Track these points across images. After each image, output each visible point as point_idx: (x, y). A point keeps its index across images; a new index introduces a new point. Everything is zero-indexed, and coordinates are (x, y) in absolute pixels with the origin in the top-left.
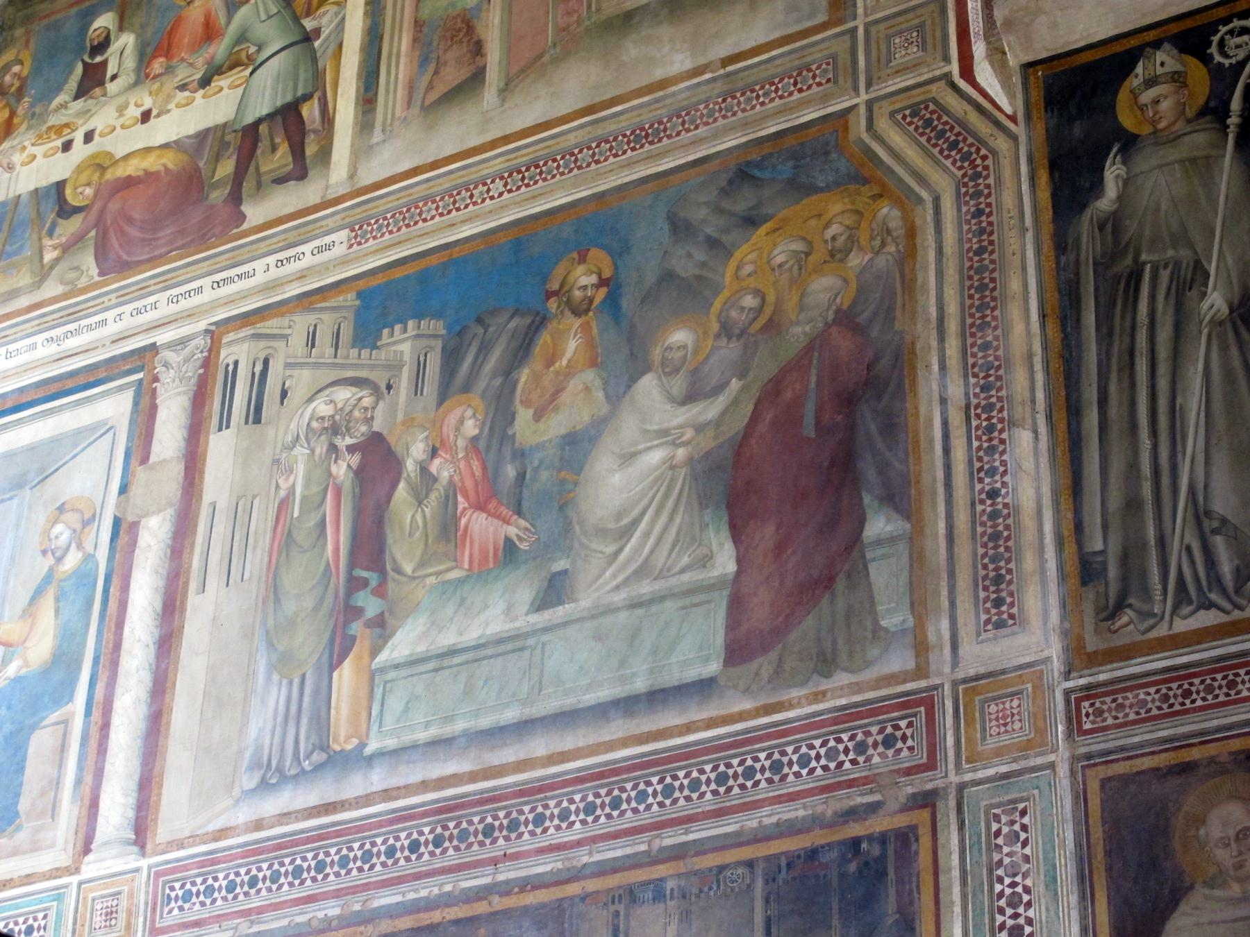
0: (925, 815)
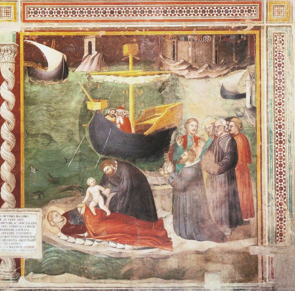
0: (257, 32)
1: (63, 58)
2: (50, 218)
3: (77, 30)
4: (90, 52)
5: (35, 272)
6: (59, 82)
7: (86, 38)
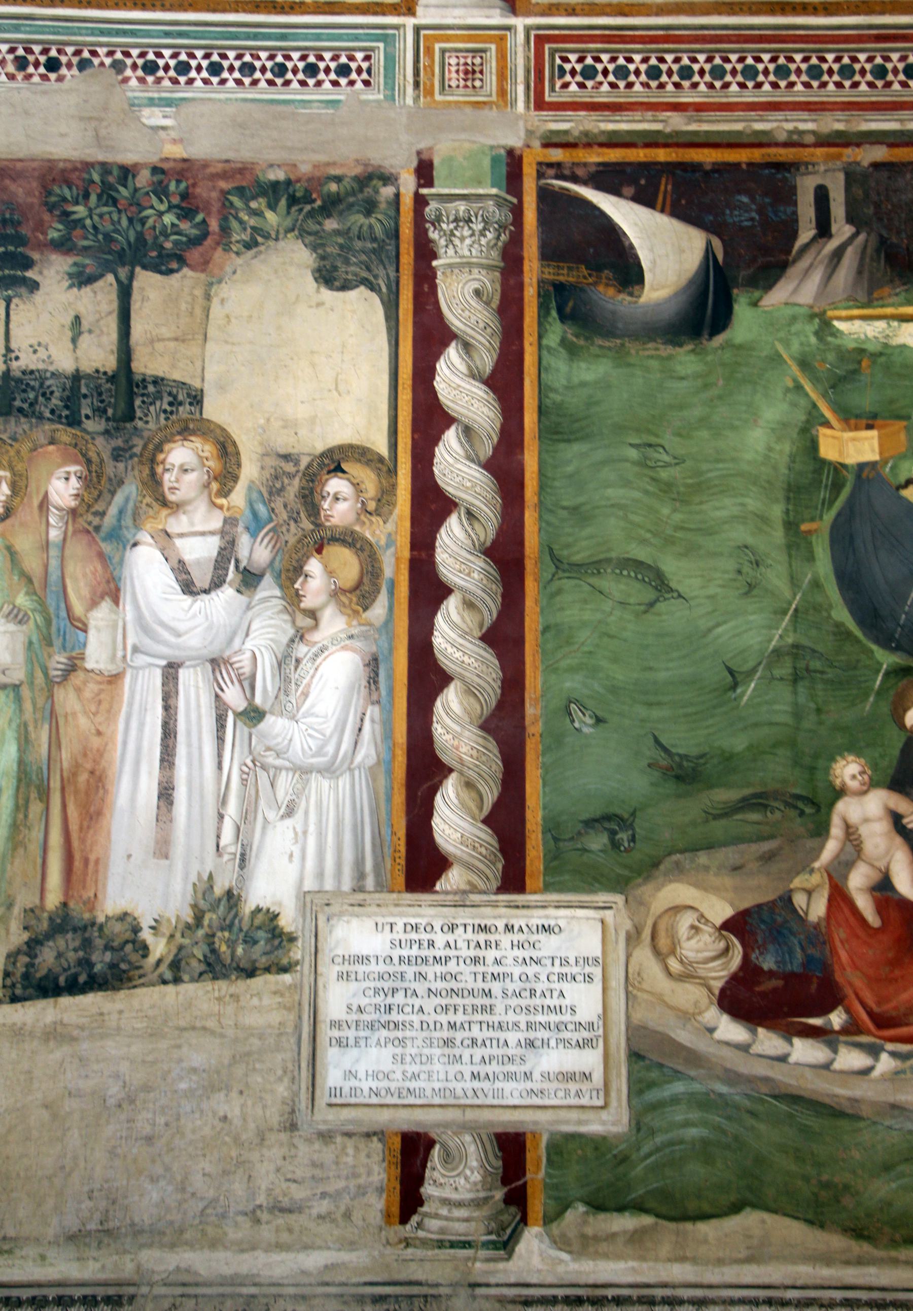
1: (709, 251)
2: (663, 942)
3: (764, 140)
4: (824, 229)
5: (598, 1206)
6: (690, 347)
7: (804, 174)
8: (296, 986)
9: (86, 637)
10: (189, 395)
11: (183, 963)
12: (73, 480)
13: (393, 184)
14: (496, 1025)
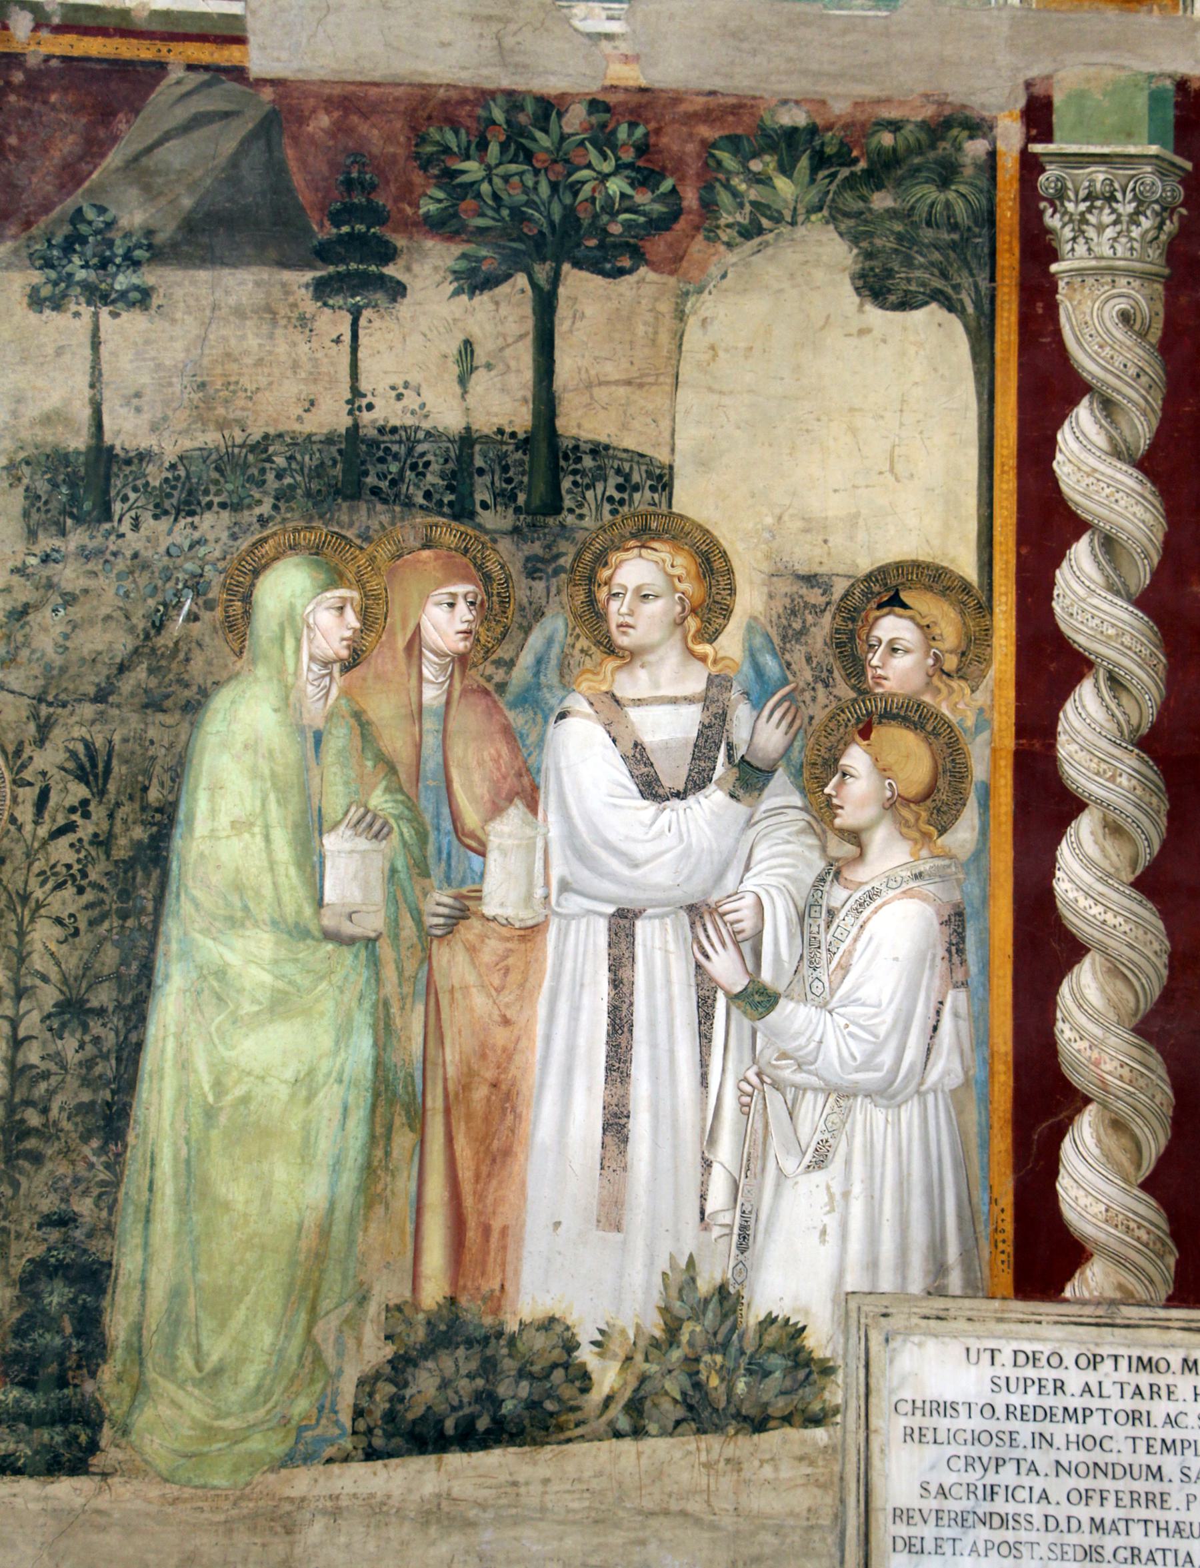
8: (834, 1449)
9: (484, 864)
10: (649, 474)
11: (648, 1404)
12: (462, 606)
13: (984, 136)
14: (1172, 1527)
